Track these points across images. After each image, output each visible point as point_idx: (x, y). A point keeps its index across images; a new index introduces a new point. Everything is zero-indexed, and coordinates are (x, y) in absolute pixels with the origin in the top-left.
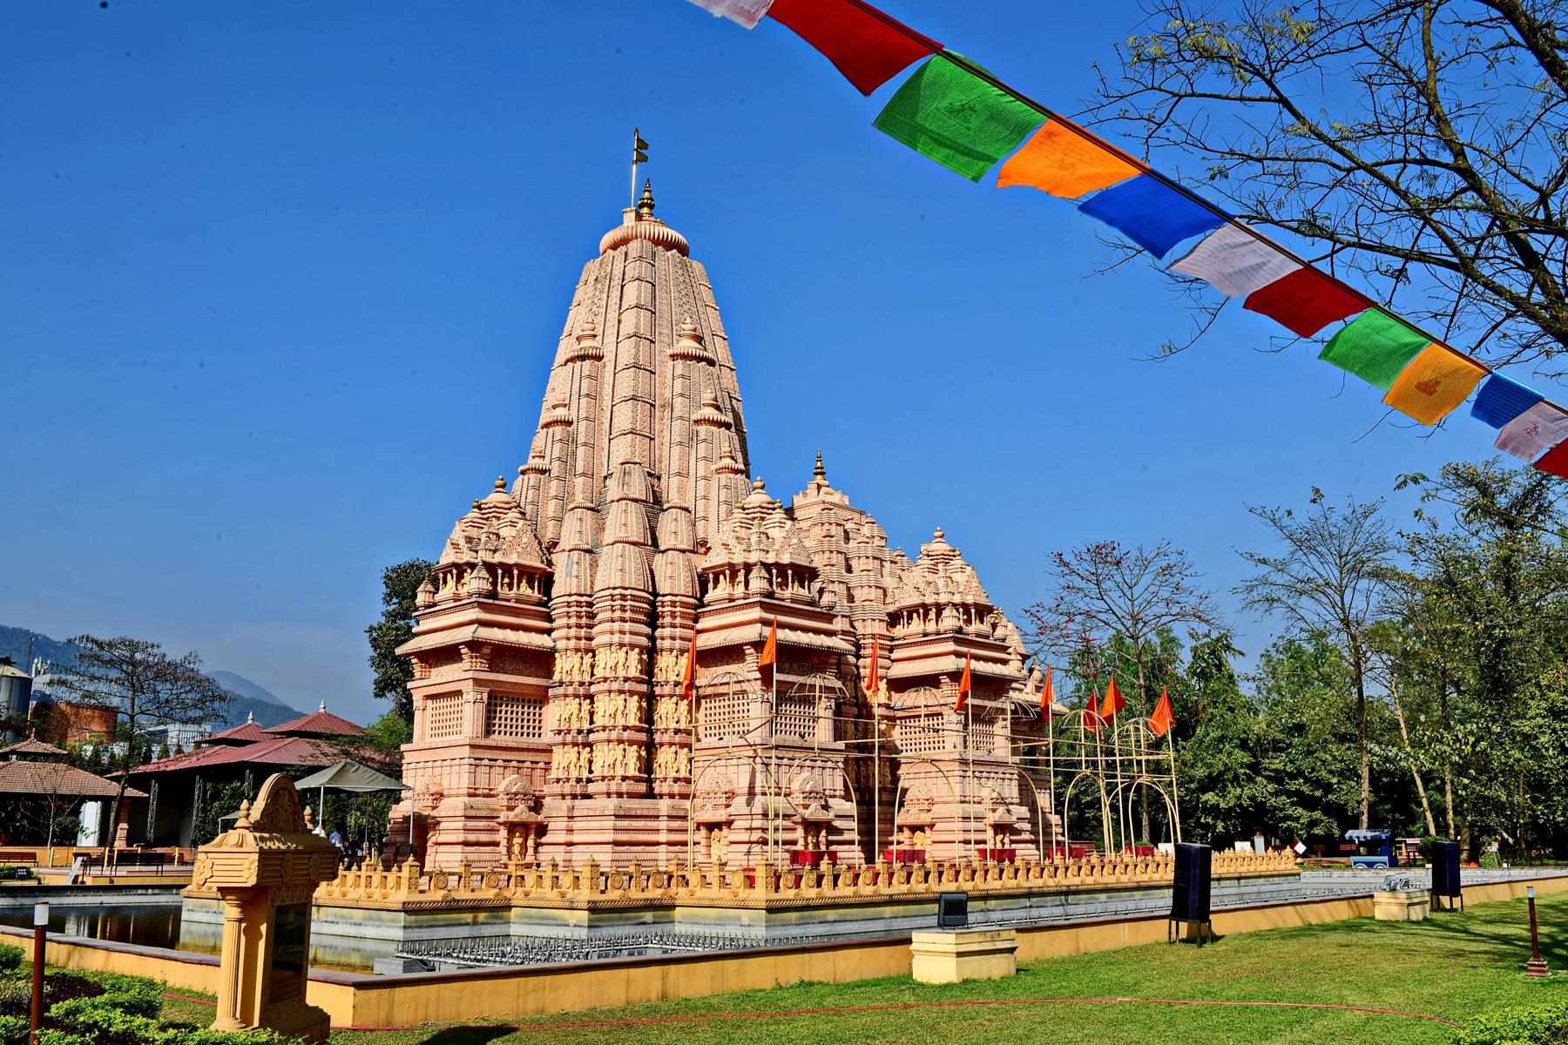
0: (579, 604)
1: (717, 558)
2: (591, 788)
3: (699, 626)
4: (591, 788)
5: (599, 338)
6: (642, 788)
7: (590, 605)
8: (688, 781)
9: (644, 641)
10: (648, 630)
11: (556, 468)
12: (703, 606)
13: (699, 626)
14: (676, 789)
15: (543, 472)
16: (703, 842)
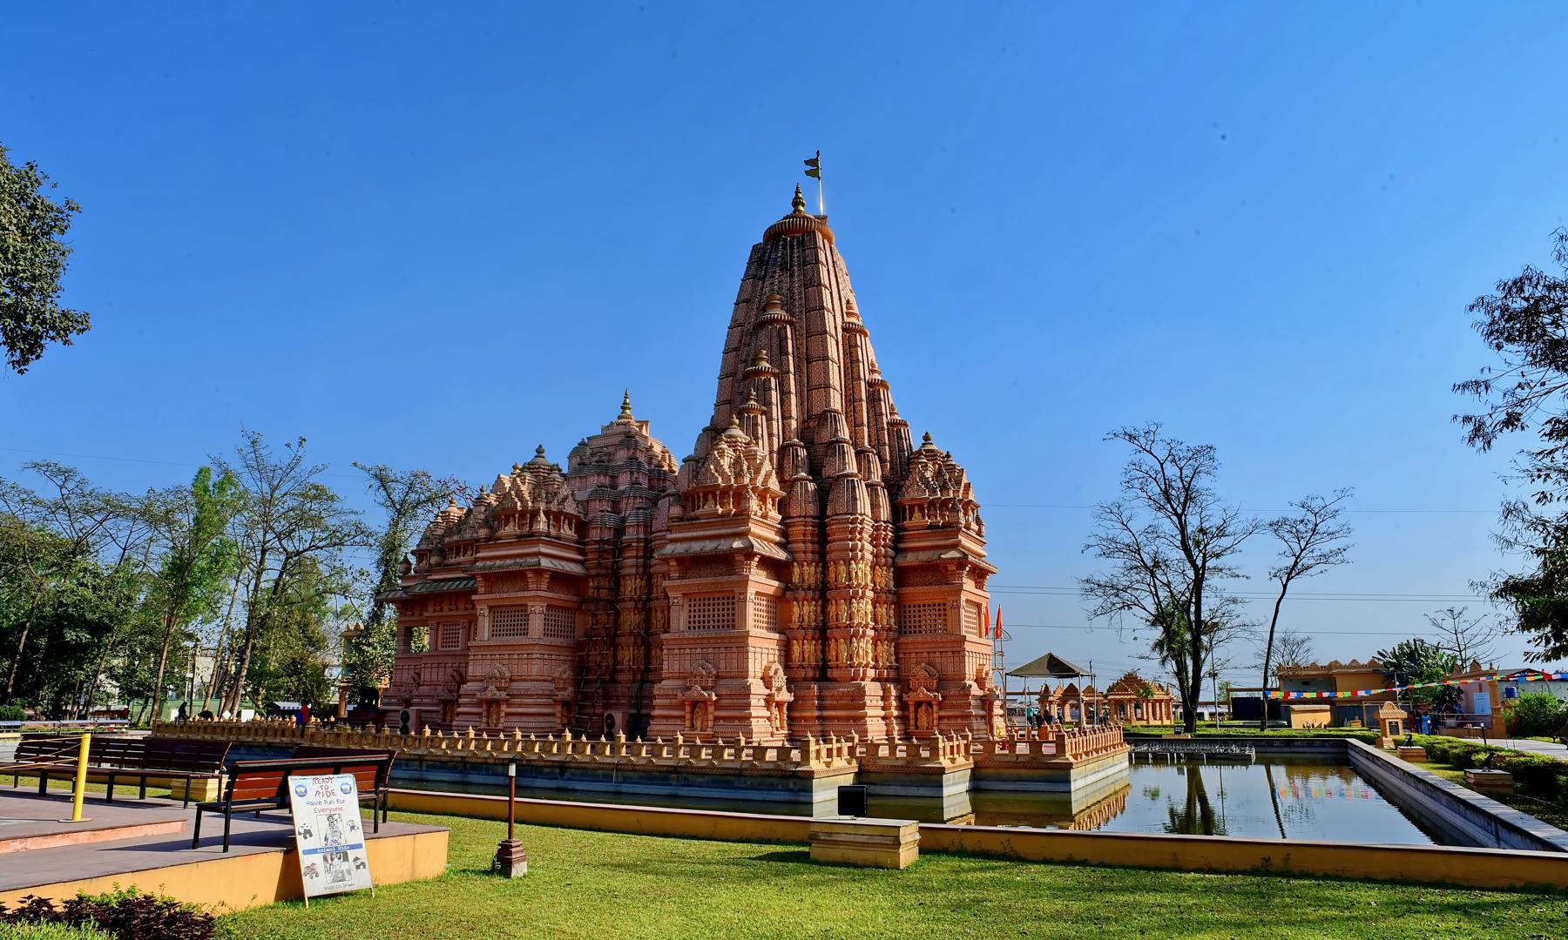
8: (897, 669)
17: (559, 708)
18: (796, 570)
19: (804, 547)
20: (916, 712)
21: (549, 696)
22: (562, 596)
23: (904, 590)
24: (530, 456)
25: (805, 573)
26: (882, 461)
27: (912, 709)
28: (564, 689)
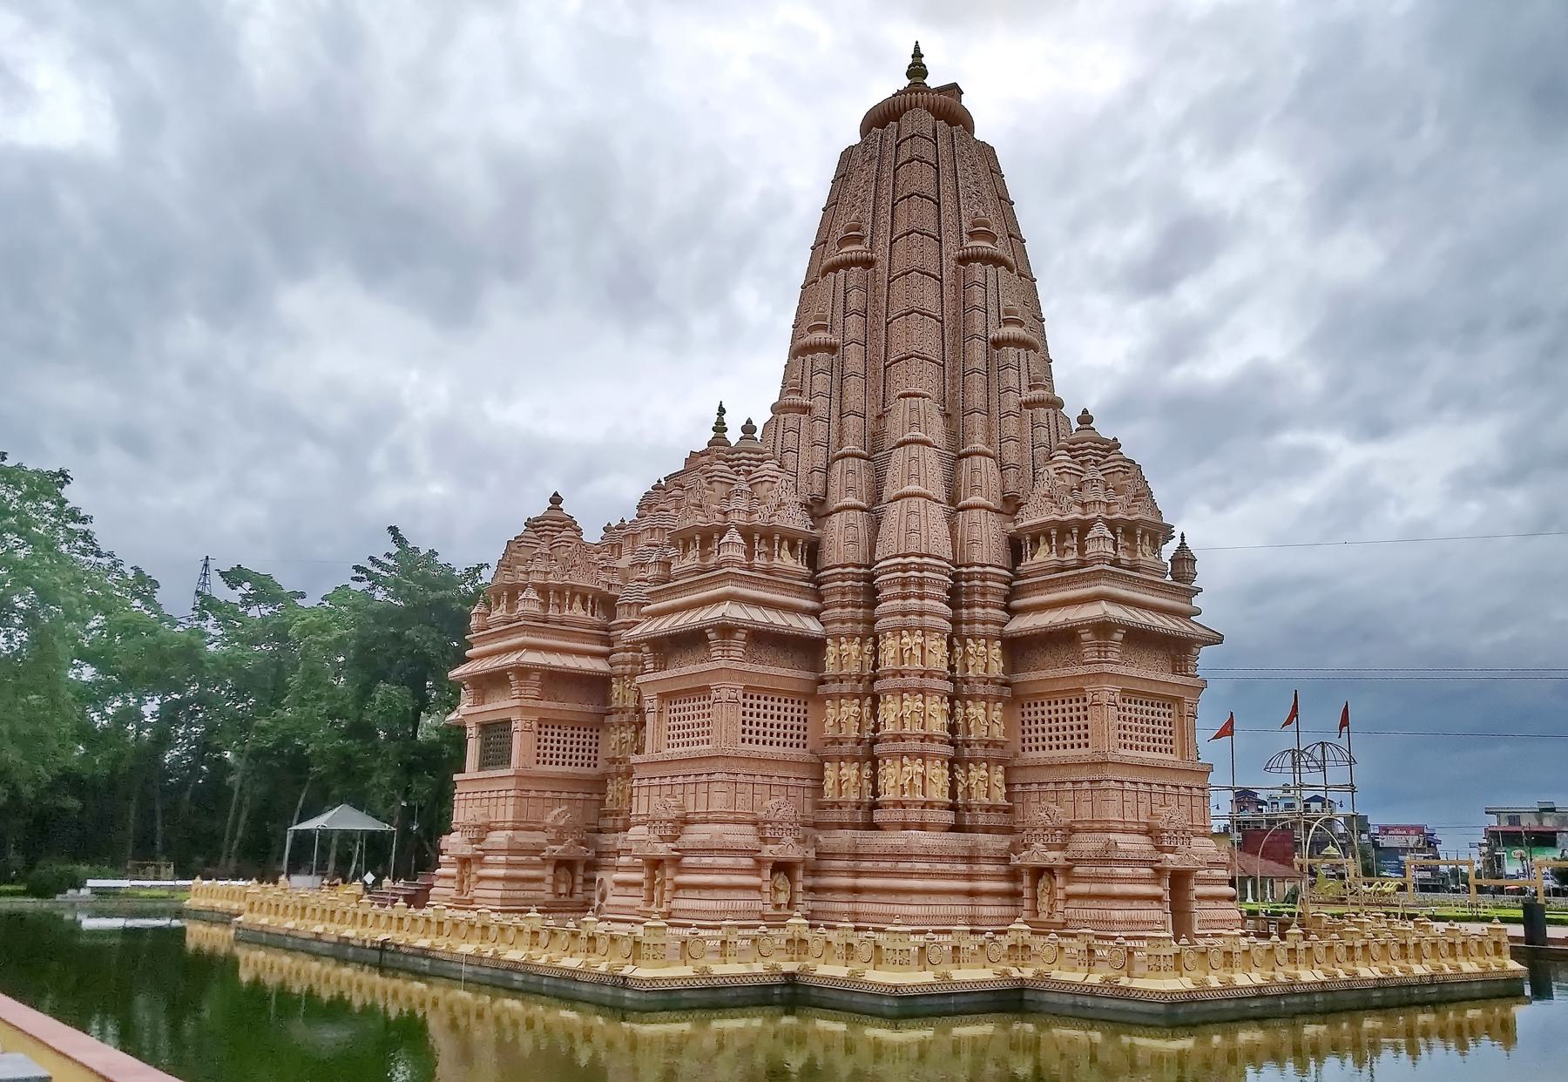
0: (857, 577)
1: (1032, 517)
2: (878, 816)
3: (1016, 603)
4: (878, 816)
5: (867, 241)
6: (949, 817)
7: (870, 578)
8: (1008, 811)
9: (949, 627)
10: (950, 612)
11: (820, 405)
12: (1018, 577)
13: (1016, 603)
14: (995, 819)
15: (806, 410)
16: (1027, 893)
17: (550, 870)
18: (831, 649)
19: (842, 613)
20: (1034, 886)
21: (537, 852)
22: (577, 707)
23: (1020, 677)
24: (540, 508)
25: (844, 657)
26: (1002, 468)
27: (1027, 880)
28: (560, 842)
